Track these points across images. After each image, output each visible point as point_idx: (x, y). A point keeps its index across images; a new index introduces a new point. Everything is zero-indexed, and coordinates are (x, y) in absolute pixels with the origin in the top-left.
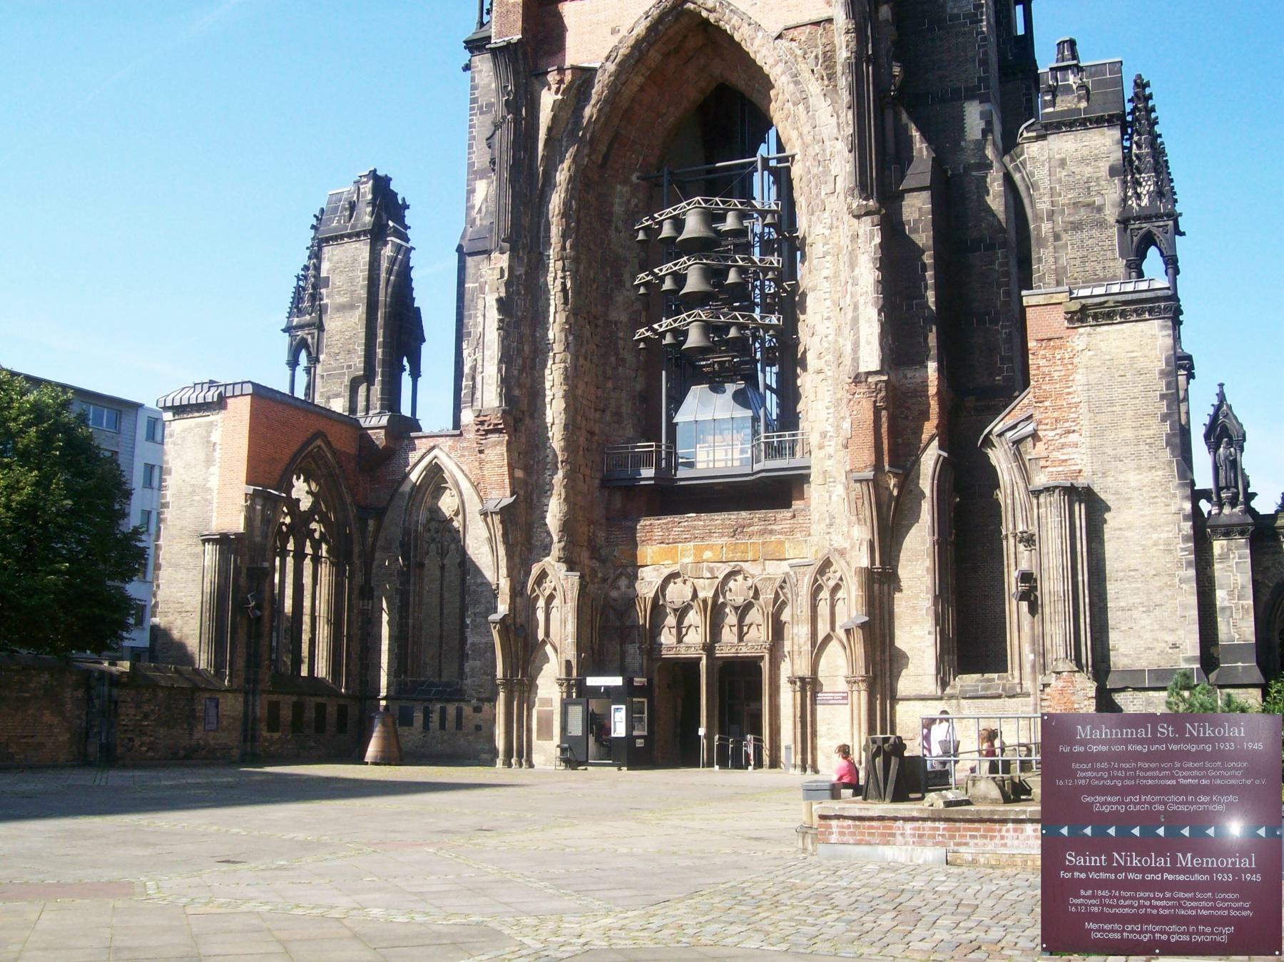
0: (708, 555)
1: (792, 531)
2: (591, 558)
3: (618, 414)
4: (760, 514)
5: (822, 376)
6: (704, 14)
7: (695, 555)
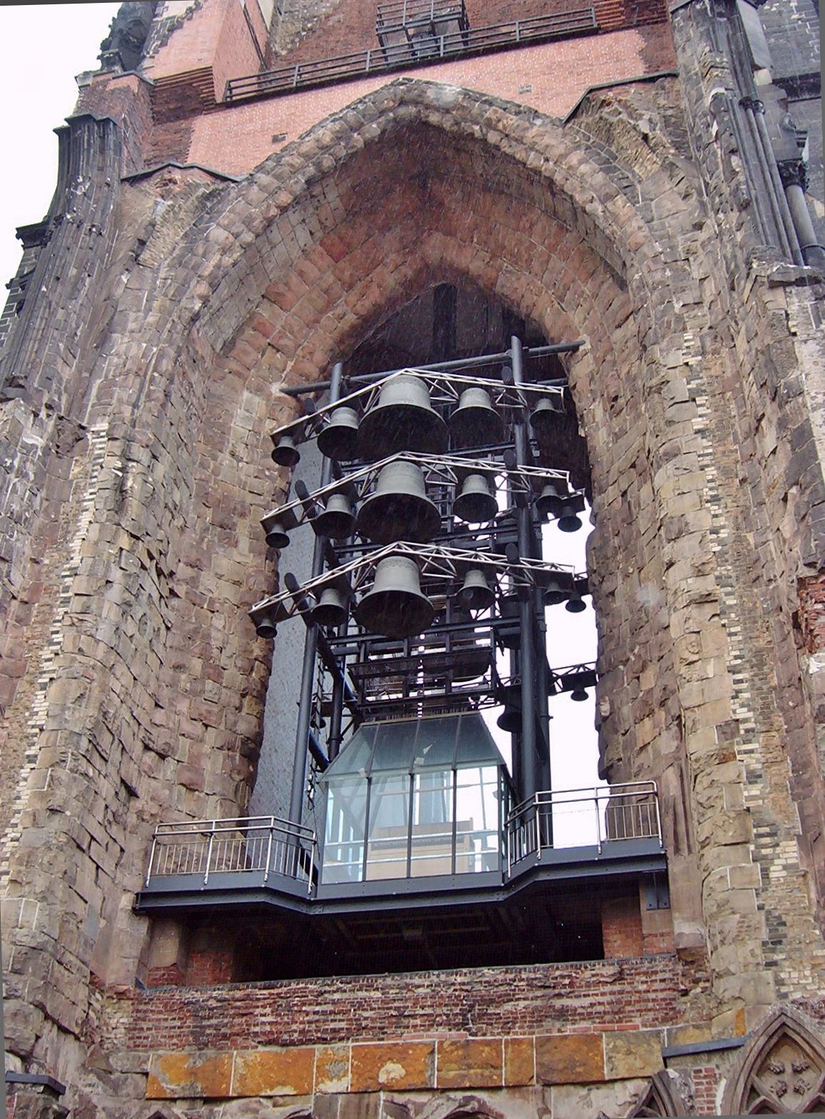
0: (392, 1071)
1: (619, 1012)
2: (84, 1068)
3: (194, 764)
4: (529, 972)
5: (709, 609)
6: (434, 118)
7: (357, 1072)
